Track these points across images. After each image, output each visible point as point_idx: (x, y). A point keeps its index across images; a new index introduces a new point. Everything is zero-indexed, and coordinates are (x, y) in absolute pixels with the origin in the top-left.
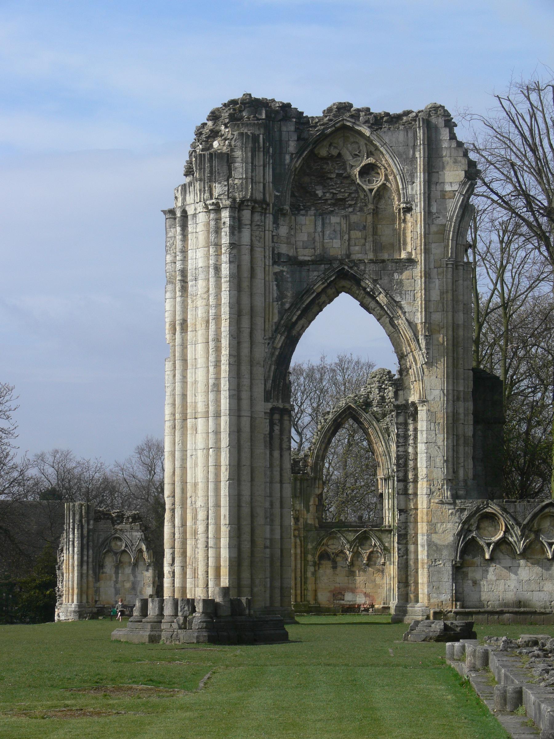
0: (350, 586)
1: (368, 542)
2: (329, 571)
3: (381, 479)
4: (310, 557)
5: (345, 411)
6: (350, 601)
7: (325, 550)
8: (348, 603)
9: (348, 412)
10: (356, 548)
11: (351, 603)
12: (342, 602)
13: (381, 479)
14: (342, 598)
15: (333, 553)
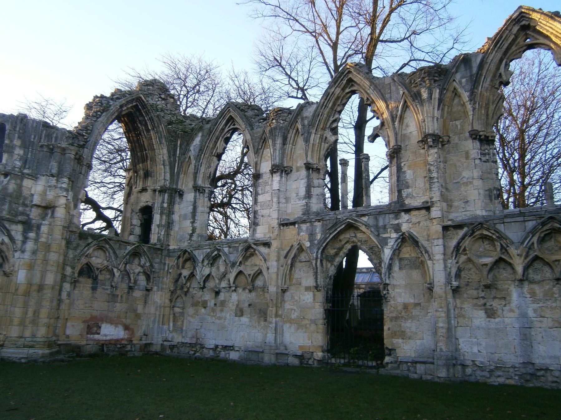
0: (110, 314)
1: (136, 261)
2: (87, 292)
3: (155, 191)
4: (69, 270)
5: (131, 101)
6: (106, 335)
7: (87, 264)
8: (104, 338)
9: (134, 104)
10: (124, 265)
11: (108, 338)
12: (96, 336)
13: (155, 191)
14: (98, 331)
15: (98, 269)
